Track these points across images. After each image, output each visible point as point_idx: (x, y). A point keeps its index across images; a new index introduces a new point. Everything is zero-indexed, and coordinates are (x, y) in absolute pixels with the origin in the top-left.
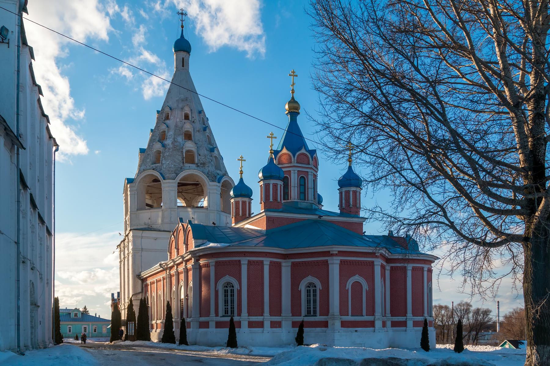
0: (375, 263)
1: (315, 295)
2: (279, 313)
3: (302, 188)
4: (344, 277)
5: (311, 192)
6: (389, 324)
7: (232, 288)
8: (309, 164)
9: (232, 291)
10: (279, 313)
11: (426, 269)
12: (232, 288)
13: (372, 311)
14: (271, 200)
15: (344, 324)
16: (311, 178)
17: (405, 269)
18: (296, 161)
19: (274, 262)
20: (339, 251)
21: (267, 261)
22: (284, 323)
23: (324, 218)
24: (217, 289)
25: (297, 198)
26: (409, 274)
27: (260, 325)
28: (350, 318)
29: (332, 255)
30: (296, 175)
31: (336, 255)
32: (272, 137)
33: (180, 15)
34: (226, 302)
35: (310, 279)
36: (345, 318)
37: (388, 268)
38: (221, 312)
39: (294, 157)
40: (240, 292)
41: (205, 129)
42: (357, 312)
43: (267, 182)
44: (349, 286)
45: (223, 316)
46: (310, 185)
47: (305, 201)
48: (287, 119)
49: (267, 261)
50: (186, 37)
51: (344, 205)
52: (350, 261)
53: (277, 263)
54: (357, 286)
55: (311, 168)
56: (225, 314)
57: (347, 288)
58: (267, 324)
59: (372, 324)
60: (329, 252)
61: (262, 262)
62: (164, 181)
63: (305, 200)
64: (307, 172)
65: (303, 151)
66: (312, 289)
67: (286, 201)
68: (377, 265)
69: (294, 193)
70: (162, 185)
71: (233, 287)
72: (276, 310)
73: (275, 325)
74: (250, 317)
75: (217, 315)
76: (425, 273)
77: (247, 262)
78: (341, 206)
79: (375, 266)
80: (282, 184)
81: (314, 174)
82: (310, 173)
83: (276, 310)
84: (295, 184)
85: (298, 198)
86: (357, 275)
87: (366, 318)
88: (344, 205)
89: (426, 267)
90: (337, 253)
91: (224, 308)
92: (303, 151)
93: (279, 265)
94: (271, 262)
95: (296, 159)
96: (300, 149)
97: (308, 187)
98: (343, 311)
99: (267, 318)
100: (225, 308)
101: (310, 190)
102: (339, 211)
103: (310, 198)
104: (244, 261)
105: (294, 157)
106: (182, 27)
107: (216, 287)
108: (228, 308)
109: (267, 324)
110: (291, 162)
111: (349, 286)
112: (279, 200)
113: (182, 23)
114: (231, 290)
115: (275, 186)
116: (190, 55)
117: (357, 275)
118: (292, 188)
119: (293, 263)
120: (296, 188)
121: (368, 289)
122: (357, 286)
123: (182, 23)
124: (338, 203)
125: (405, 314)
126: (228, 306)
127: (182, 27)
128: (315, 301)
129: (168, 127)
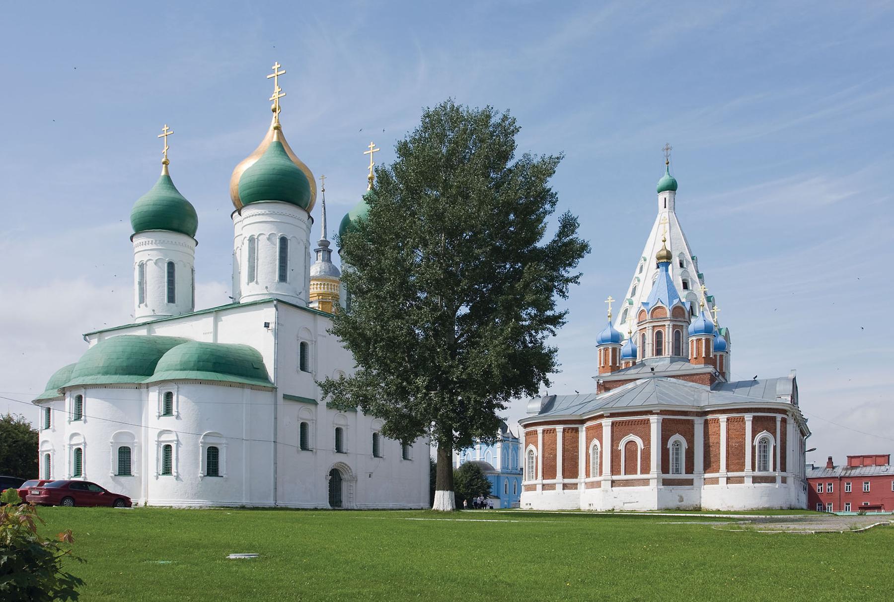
13: (646, 469)
17: (717, 421)
20: (611, 414)
21: (559, 428)
23: (656, 374)
25: (650, 354)
30: (651, 331)
44: (622, 447)
47: (661, 357)
49: (559, 428)
61: (555, 430)
85: (653, 354)
97: (665, 341)
111: (622, 447)
116: (675, 194)
120: (650, 345)
122: (677, 444)
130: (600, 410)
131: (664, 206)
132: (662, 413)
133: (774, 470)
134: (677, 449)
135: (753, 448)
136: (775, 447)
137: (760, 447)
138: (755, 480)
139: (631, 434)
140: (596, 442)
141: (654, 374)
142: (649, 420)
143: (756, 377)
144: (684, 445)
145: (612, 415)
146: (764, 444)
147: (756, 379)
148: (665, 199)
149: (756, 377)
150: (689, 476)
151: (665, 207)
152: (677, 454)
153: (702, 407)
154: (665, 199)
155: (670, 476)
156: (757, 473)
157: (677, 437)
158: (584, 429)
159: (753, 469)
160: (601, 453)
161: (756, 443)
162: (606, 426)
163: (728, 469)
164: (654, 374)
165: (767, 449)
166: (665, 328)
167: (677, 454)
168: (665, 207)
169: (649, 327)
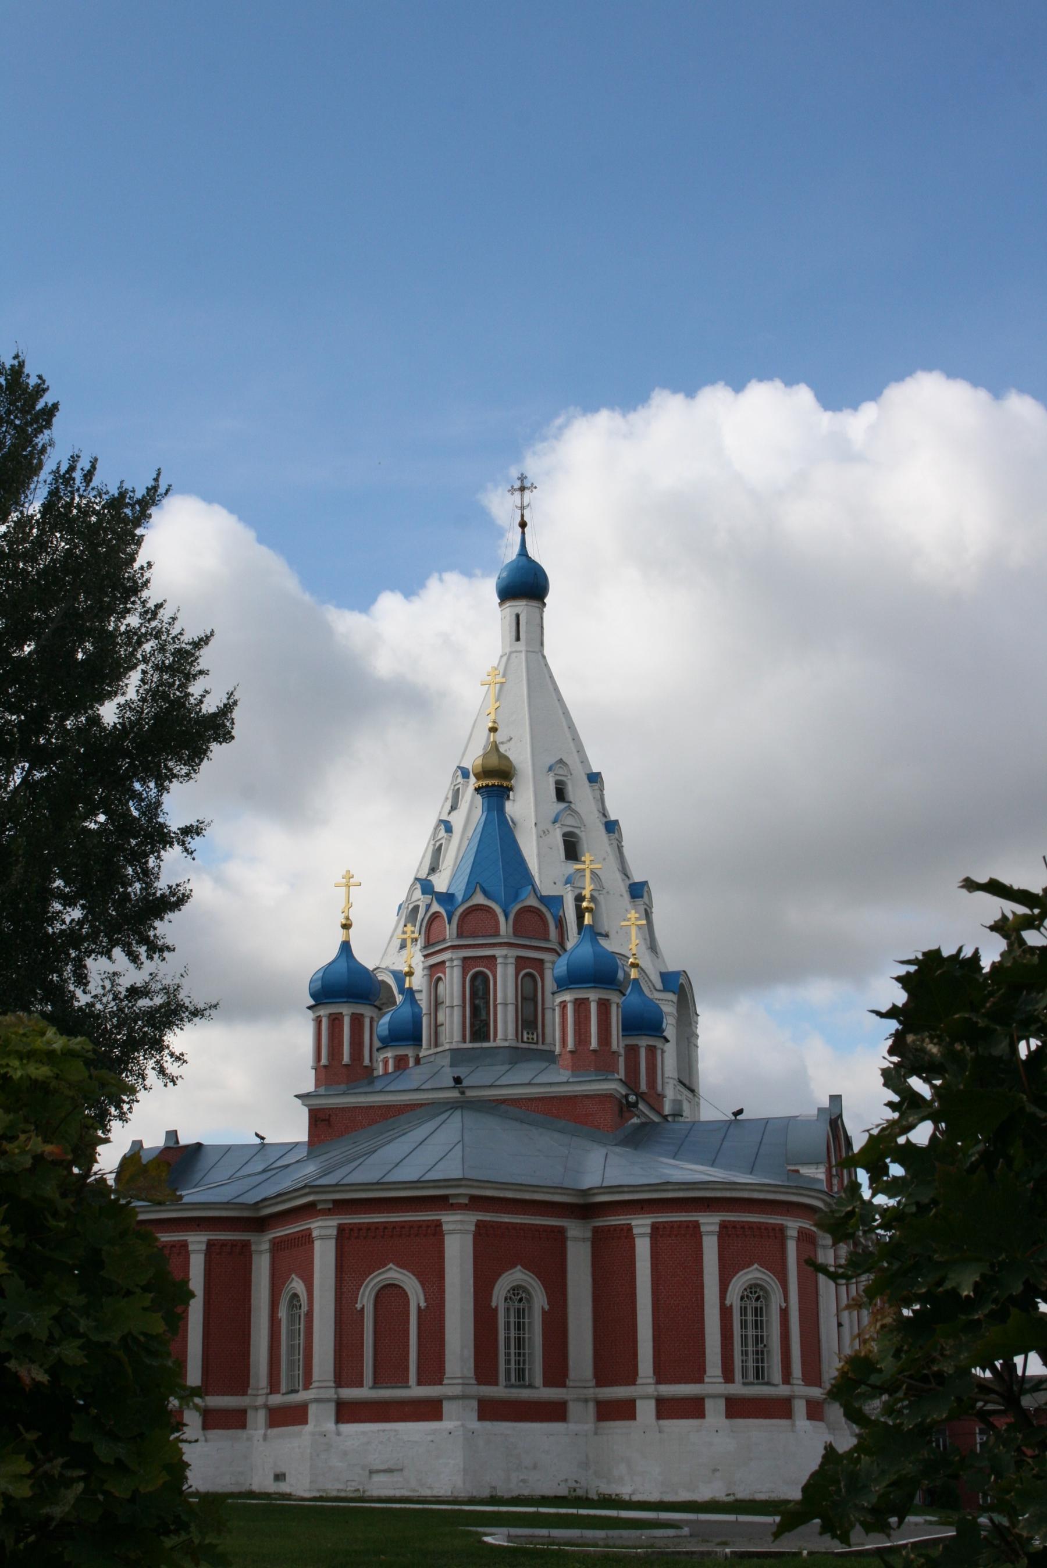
0: (445, 1227)
8: (497, 934)
10: (240, 1383)
17: (627, 1234)
18: (455, 931)
19: (223, 1244)
20: (335, 1202)
22: (573, 1409)
23: (470, 1093)
25: (457, 1036)
26: (643, 1248)
28: (364, 1393)
30: (457, 973)
31: (328, 1212)
33: (517, 494)
36: (350, 1393)
44: (366, 1299)
47: (485, 1045)
52: (369, 1227)
53: (233, 1244)
61: (184, 1245)
64: (493, 958)
68: (452, 1232)
79: (447, 1237)
82: (499, 960)
84: (505, 997)
87: (417, 1391)
90: (331, 1206)
93: (244, 1251)
94: (210, 1244)
97: (495, 999)
103: (500, 1035)
106: (523, 525)
113: (522, 516)
116: (544, 604)
118: (499, 1008)
120: (457, 1012)
121: (423, 1305)
123: (522, 516)
125: (631, 1377)
127: (523, 525)
130: (307, 1190)
131: (514, 634)
132: (477, 1203)
133: (787, 1379)
134: (520, 1313)
135: (726, 1312)
136: (784, 1313)
137: (743, 1311)
138: (736, 1408)
139: (391, 1265)
140: (297, 1285)
141: (463, 1093)
142: (438, 1224)
143: (740, 1112)
144: (540, 1300)
145: (341, 1206)
146: (754, 1304)
147: (739, 1117)
148: (518, 616)
149: (740, 1112)
151: (518, 639)
152: (519, 1327)
153: (585, 1192)
154: (518, 616)
155: (498, 1391)
156: (737, 1389)
157: (517, 1276)
158: (266, 1246)
159: (728, 1376)
160: (309, 1315)
161: (733, 1297)
162: (322, 1238)
163: (661, 1375)
164: (463, 1093)
165: (764, 1318)
166: (496, 965)
167: (519, 1327)
168: (518, 639)
169: (451, 960)
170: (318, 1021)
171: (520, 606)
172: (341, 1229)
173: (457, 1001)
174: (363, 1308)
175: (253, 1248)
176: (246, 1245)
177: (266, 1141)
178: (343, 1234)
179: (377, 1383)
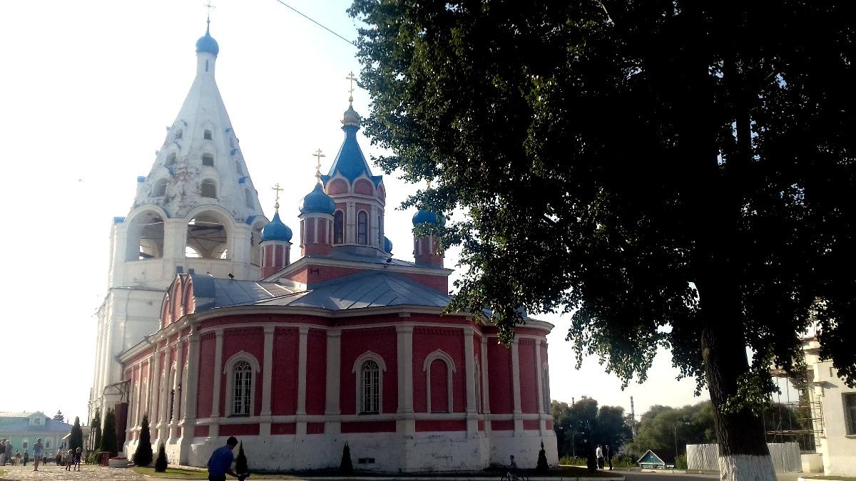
1: (376, 381)
2: (321, 410)
3: (362, 227)
4: (420, 351)
5: (374, 233)
6: (488, 425)
7: (249, 371)
8: (371, 194)
9: (249, 375)
10: (321, 410)
11: (538, 343)
12: (249, 371)
13: (462, 405)
14: (316, 241)
15: (422, 426)
16: (374, 214)
19: (317, 331)
21: (304, 329)
24: (224, 372)
25: (354, 240)
27: (290, 428)
28: (428, 416)
29: (402, 319)
30: (354, 209)
31: (408, 319)
32: (319, 155)
34: (238, 393)
35: (369, 355)
37: (484, 340)
38: (229, 409)
39: (351, 184)
40: (260, 377)
41: (233, 153)
42: (441, 405)
43: (311, 215)
44: (427, 365)
45: (232, 416)
46: (374, 223)
48: (341, 137)
49: (304, 329)
50: (212, 35)
51: (420, 252)
53: (320, 331)
54: (439, 365)
55: (374, 200)
56: (236, 412)
57: (424, 370)
58: (302, 428)
59: (461, 425)
60: (397, 315)
61: (297, 330)
62: (168, 220)
63: (366, 243)
64: (370, 205)
65: (364, 176)
66: (372, 371)
67: (338, 245)
69: (350, 233)
70: (165, 225)
71: (250, 368)
72: (317, 403)
73: (315, 428)
74: (275, 417)
75: (222, 414)
76: (538, 348)
77: (273, 330)
78: (416, 253)
79: (466, 337)
80: (333, 220)
81: (379, 208)
82: (373, 207)
83: (317, 403)
86: (439, 349)
87: (453, 416)
88: (420, 252)
89: (538, 339)
90: (409, 316)
91: (234, 403)
92: (364, 176)
94: (311, 330)
95: (353, 186)
96: (358, 174)
98: (419, 405)
99: (302, 417)
100: (236, 403)
101: (373, 230)
102: (413, 260)
104: (269, 328)
105: (351, 184)
106: (209, 22)
107: (223, 370)
108: (240, 403)
109: (302, 428)
110: (346, 192)
111: (427, 365)
112: (327, 241)
114: (247, 373)
115: (322, 222)
117: (439, 349)
119: (343, 331)
121: (455, 371)
122: (439, 365)
124: (412, 248)
125: (511, 409)
126: (240, 399)
127: (209, 22)
128: (376, 390)
129: (180, 147)
141: (385, 267)
150: (459, 416)
154: (207, 62)
166: (370, 209)
168: (207, 70)
169: (351, 203)
170: (302, 222)
171: (206, 56)
172: (415, 329)
173: (354, 223)
174: (426, 370)
175: (328, 334)
176: (324, 333)
177: (234, 278)
178: (417, 331)
179: (433, 411)
